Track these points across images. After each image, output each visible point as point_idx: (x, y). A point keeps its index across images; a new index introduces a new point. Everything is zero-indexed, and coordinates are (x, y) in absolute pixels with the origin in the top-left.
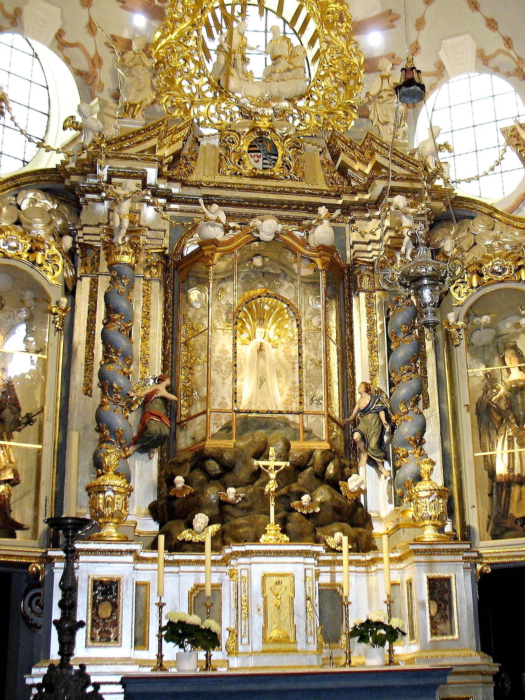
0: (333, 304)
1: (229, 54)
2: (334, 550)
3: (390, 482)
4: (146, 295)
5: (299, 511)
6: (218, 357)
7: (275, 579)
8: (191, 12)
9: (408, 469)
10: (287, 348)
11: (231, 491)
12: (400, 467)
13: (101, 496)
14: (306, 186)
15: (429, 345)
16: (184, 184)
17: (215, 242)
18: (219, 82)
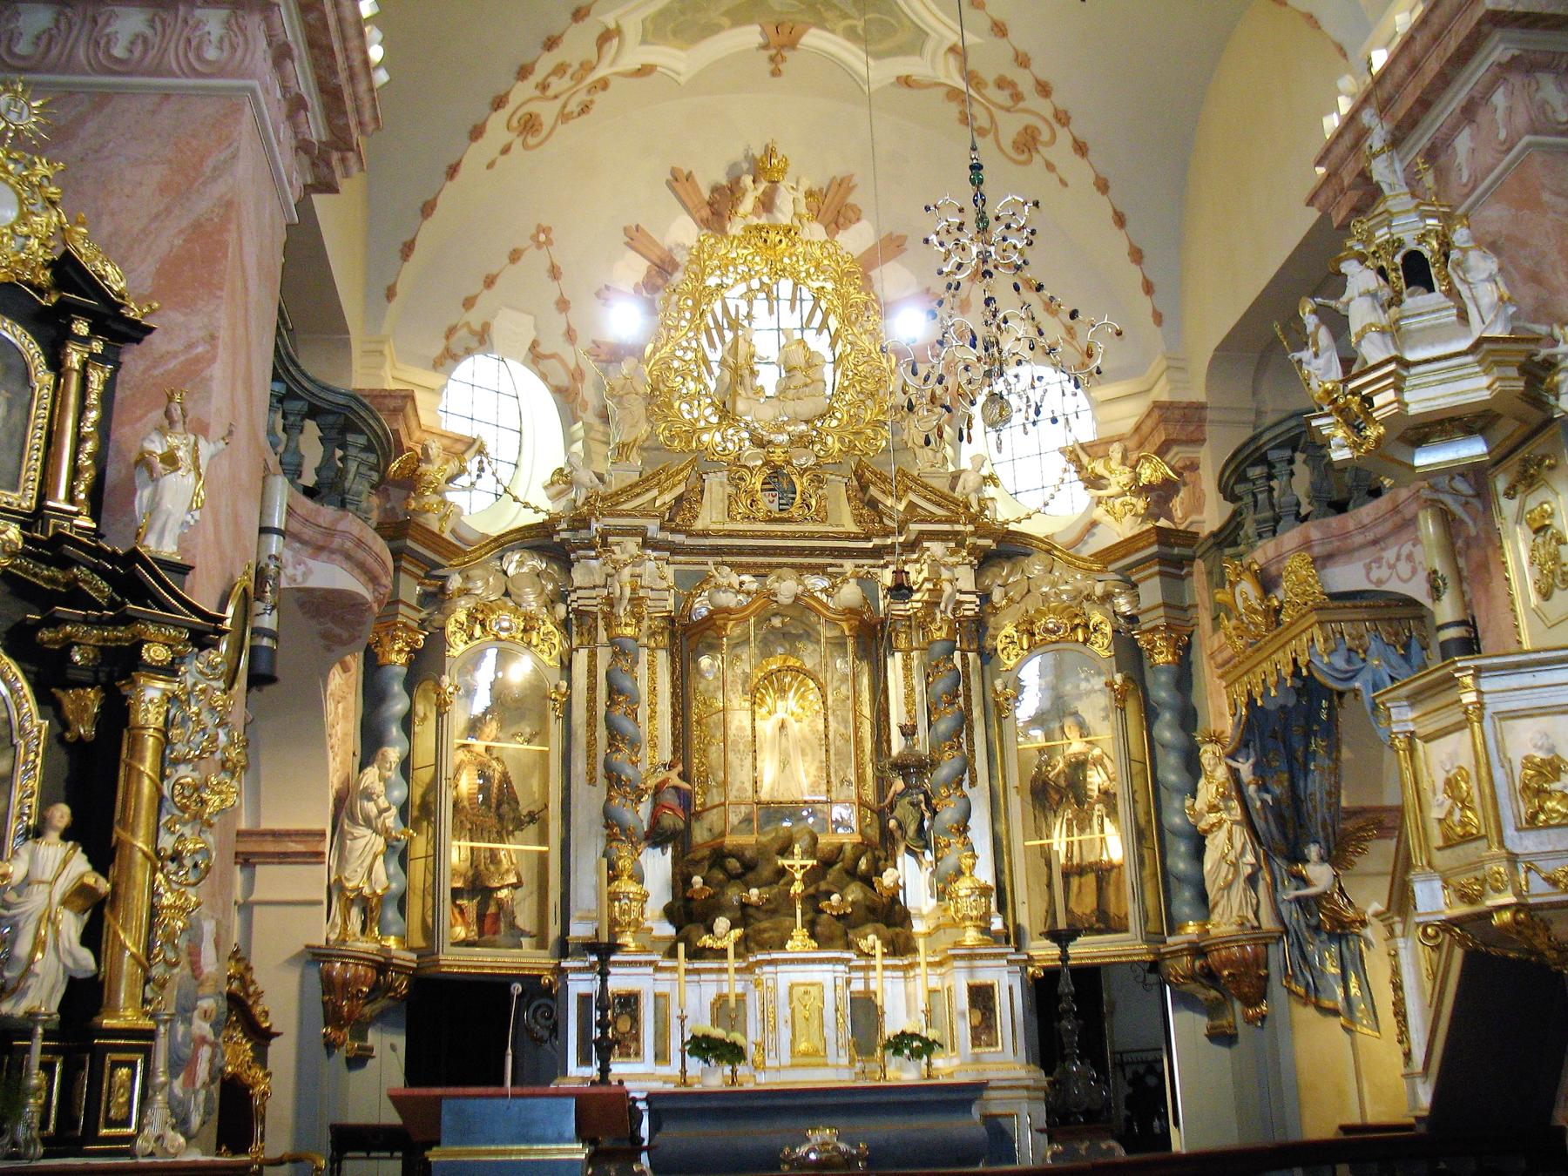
0: (865, 668)
1: (735, 370)
3: (932, 873)
4: (651, 665)
7: (802, 989)
11: (754, 892)
14: (830, 529)
16: (690, 534)
17: (727, 611)
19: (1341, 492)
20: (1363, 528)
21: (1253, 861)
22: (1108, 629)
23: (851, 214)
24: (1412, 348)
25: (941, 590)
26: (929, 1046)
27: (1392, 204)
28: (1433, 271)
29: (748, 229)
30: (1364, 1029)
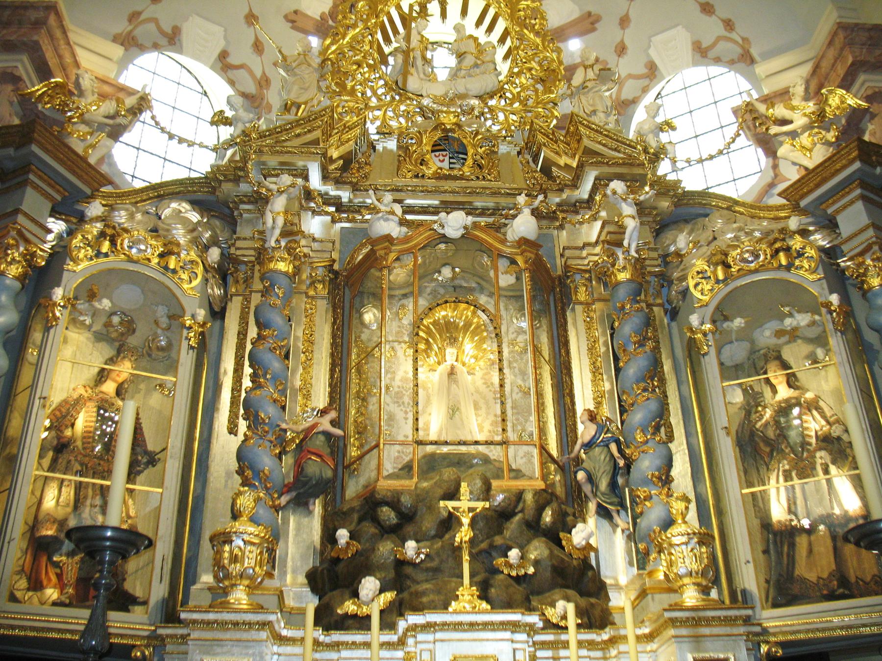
2: (556, 626)
5: (506, 572)
6: (399, 387)
8: (365, 17)
9: (653, 515)
10: (486, 374)
12: (641, 513)
13: (227, 548)
15: (667, 366)
18: (397, 82)
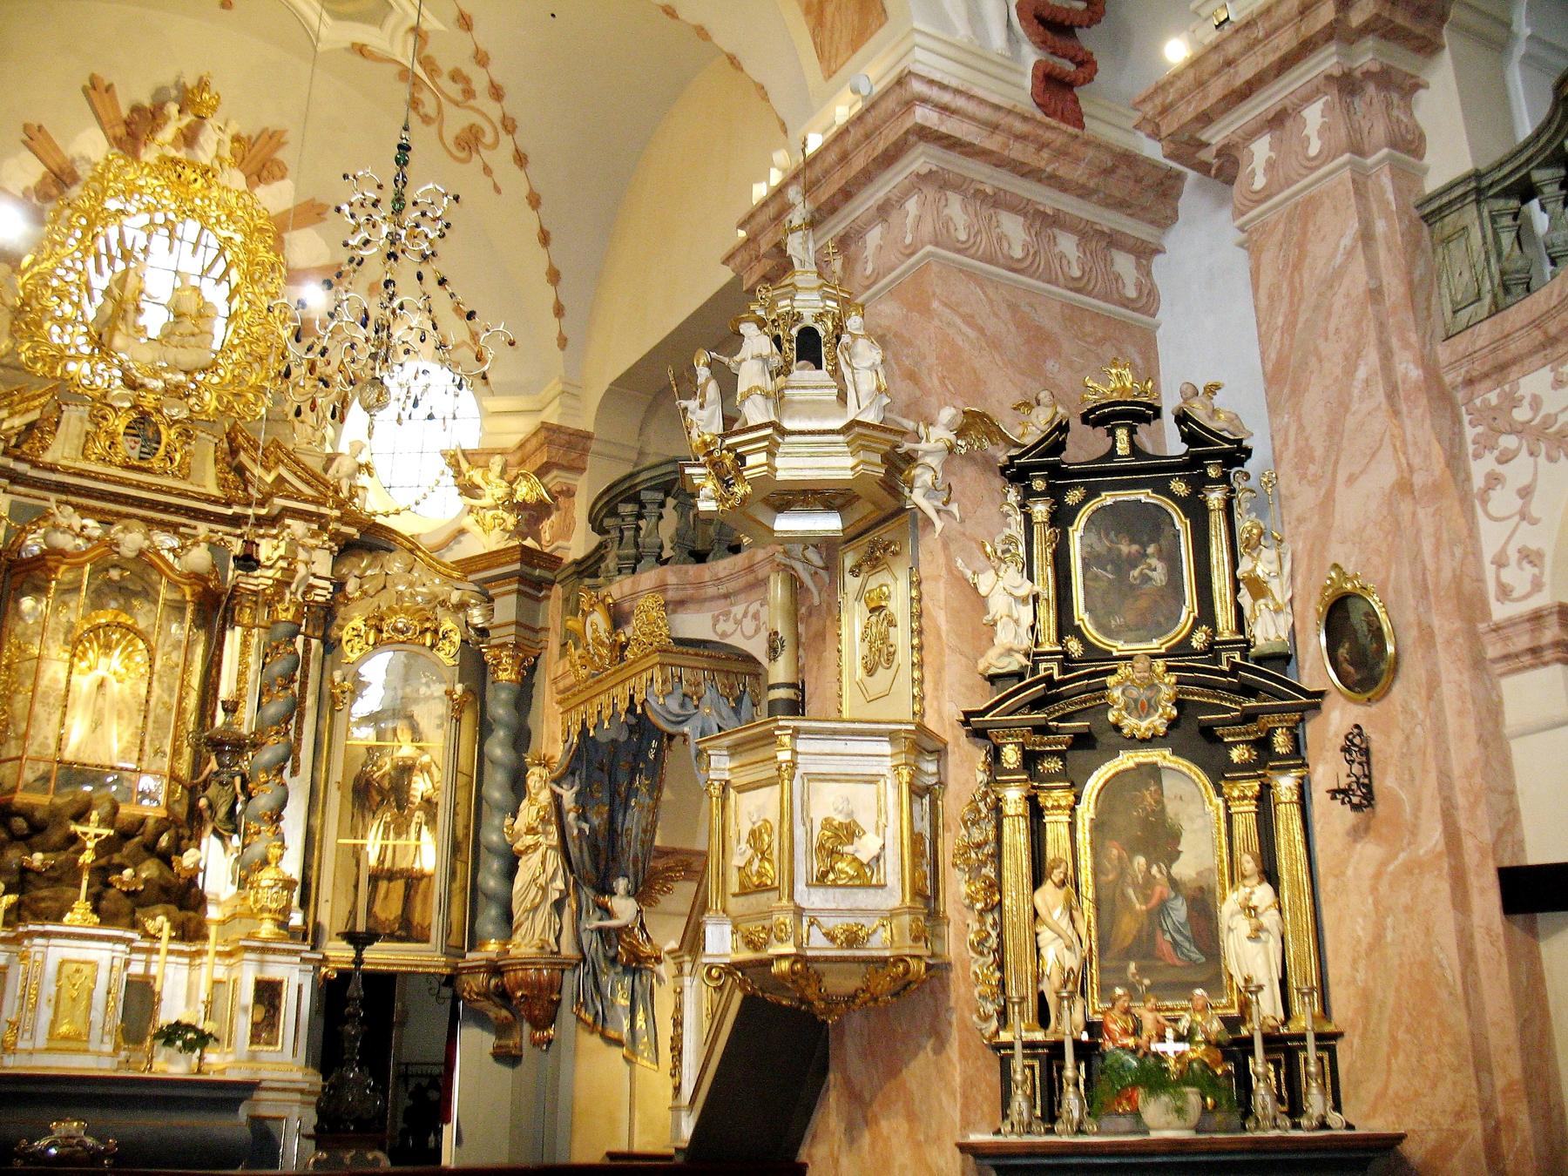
1: (120, 304)
2: (154, 937)
3: (237, 860)
9: (258, 848)
14: (190, 488)
16: (35, 465)
17: (62, 553)
19: (705, 544)
20: (718, 581)
21: (562, 887)
22: (457, 638)
23: (276, 169)
24: (791, 417)
25: (295, 571)
26: (203, 1039)
27: (799, 279)
28: (824, 350)
29: (163, 159)
30: (644, 1062)
